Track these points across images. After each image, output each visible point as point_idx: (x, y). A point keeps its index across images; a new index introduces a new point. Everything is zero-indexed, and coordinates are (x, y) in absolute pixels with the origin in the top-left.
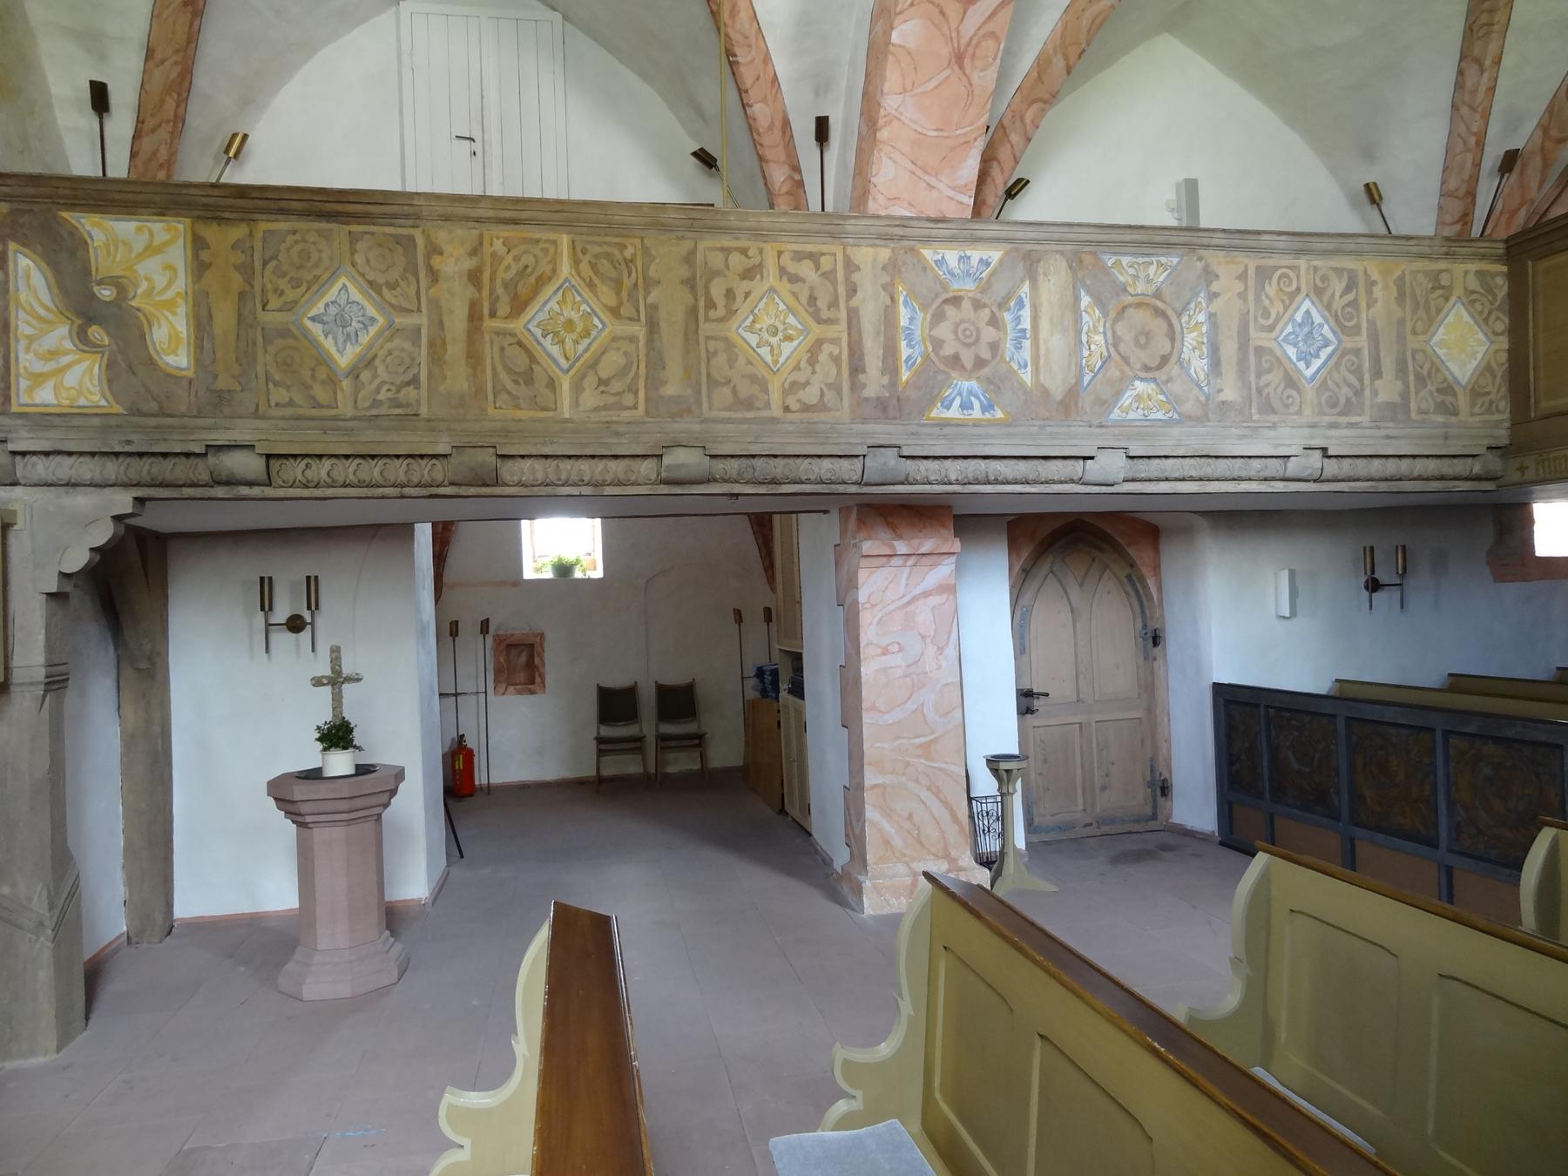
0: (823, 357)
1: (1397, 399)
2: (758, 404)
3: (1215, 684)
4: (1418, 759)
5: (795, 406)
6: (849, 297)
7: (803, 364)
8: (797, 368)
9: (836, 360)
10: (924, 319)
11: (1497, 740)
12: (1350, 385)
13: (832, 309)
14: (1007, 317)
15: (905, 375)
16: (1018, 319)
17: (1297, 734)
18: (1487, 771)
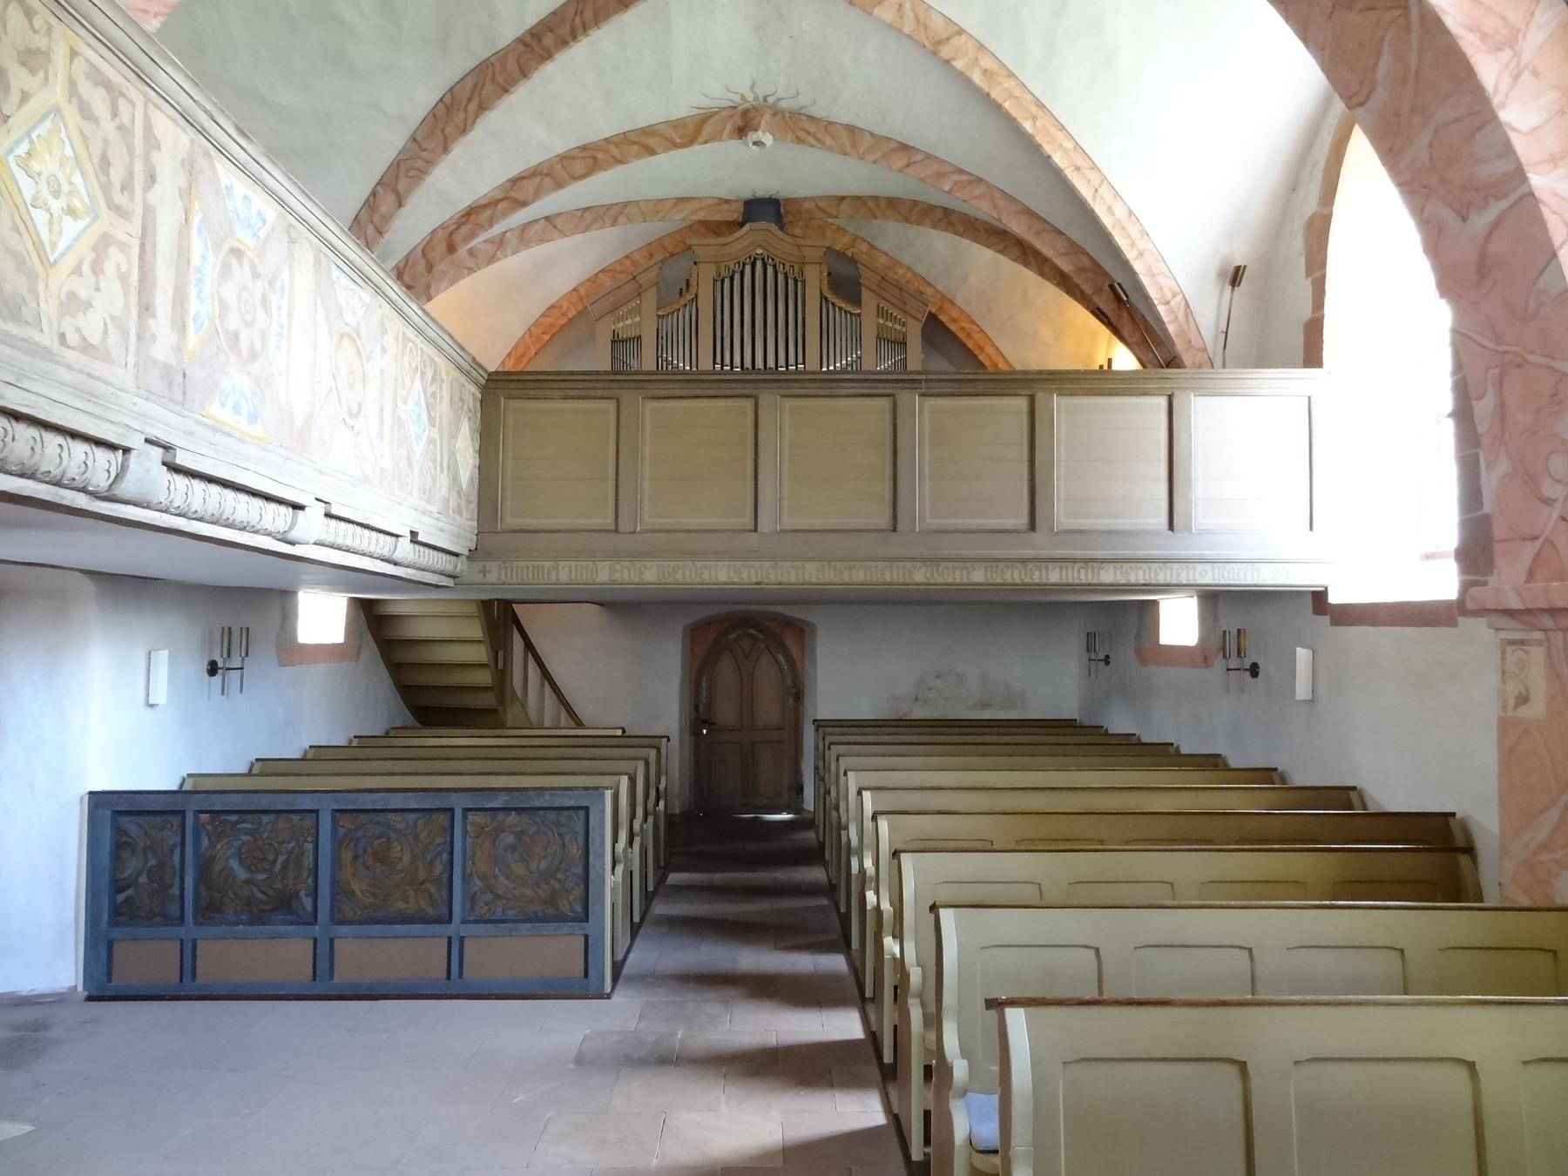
0: (109, 267)
1: (447, 496)
2: (27, 313)
3: (91, 793)
4: (428, 841)
5: (72, 338)
6: (146, 189)
7: (86, 268)
8: (77, 271)
9: (123, 278)
10: (215, 265)
11: (520, 810)
12: (432, 475)
13: (125, 193)
14: (274, 300)
15: (193, 340)
16: (279, 307)
17: (246, 838)
18: (510, 839)
